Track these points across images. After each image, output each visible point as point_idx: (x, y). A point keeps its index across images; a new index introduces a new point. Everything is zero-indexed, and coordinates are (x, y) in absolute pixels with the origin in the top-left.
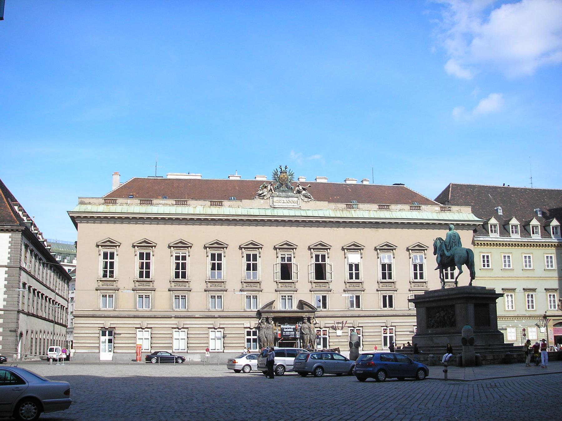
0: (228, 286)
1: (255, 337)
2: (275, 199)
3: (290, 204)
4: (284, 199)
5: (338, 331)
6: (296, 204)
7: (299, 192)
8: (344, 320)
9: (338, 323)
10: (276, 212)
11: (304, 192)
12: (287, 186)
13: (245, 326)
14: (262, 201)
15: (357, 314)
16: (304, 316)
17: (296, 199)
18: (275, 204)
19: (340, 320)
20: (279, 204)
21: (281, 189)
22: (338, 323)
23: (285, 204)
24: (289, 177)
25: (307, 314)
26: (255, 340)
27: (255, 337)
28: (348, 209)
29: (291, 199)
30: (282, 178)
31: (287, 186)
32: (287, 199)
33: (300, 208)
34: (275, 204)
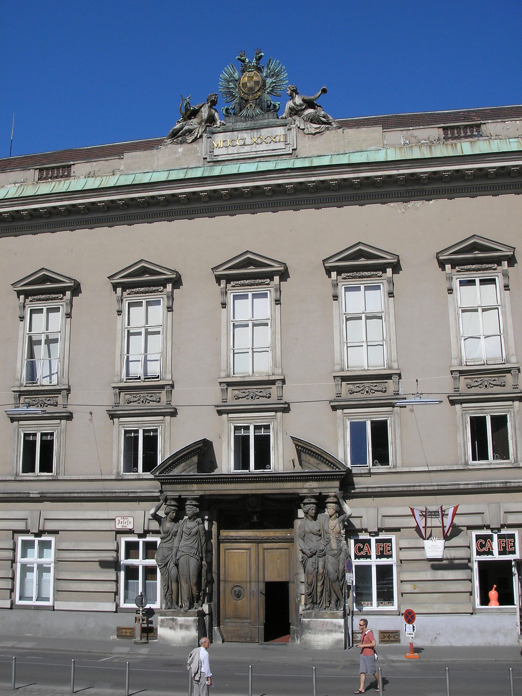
0: (76, 402)
1: (151, 562)
2: (219, 139)
3: (263, 147)
4: (245, 135)
5: (427, 543)
6: (281, 145)
7: (295, 112)
8: (448, 503)
9: (426, 514)
10: (217, 171)
11: (310, 111)
12: (259, 102)
13: (119, 527)
14: (180, 149)
15: (497, 479)
16: (304, 492)
17: (280, 131)
18: (217, 152)
19: (432, 503)
20: (231, 150)
21: (244, 112)
22: (426, 514)
23: (246, 149)
24: (269, 81)
25: (314, 484)
26: (150, 572)
27: (151, 562)
28: (450, 141)
29: (265, 132)
30: (245, 85)
31: (259, 102)
32: (255, 133)
33: (293, 154)
34: (217, 152)
